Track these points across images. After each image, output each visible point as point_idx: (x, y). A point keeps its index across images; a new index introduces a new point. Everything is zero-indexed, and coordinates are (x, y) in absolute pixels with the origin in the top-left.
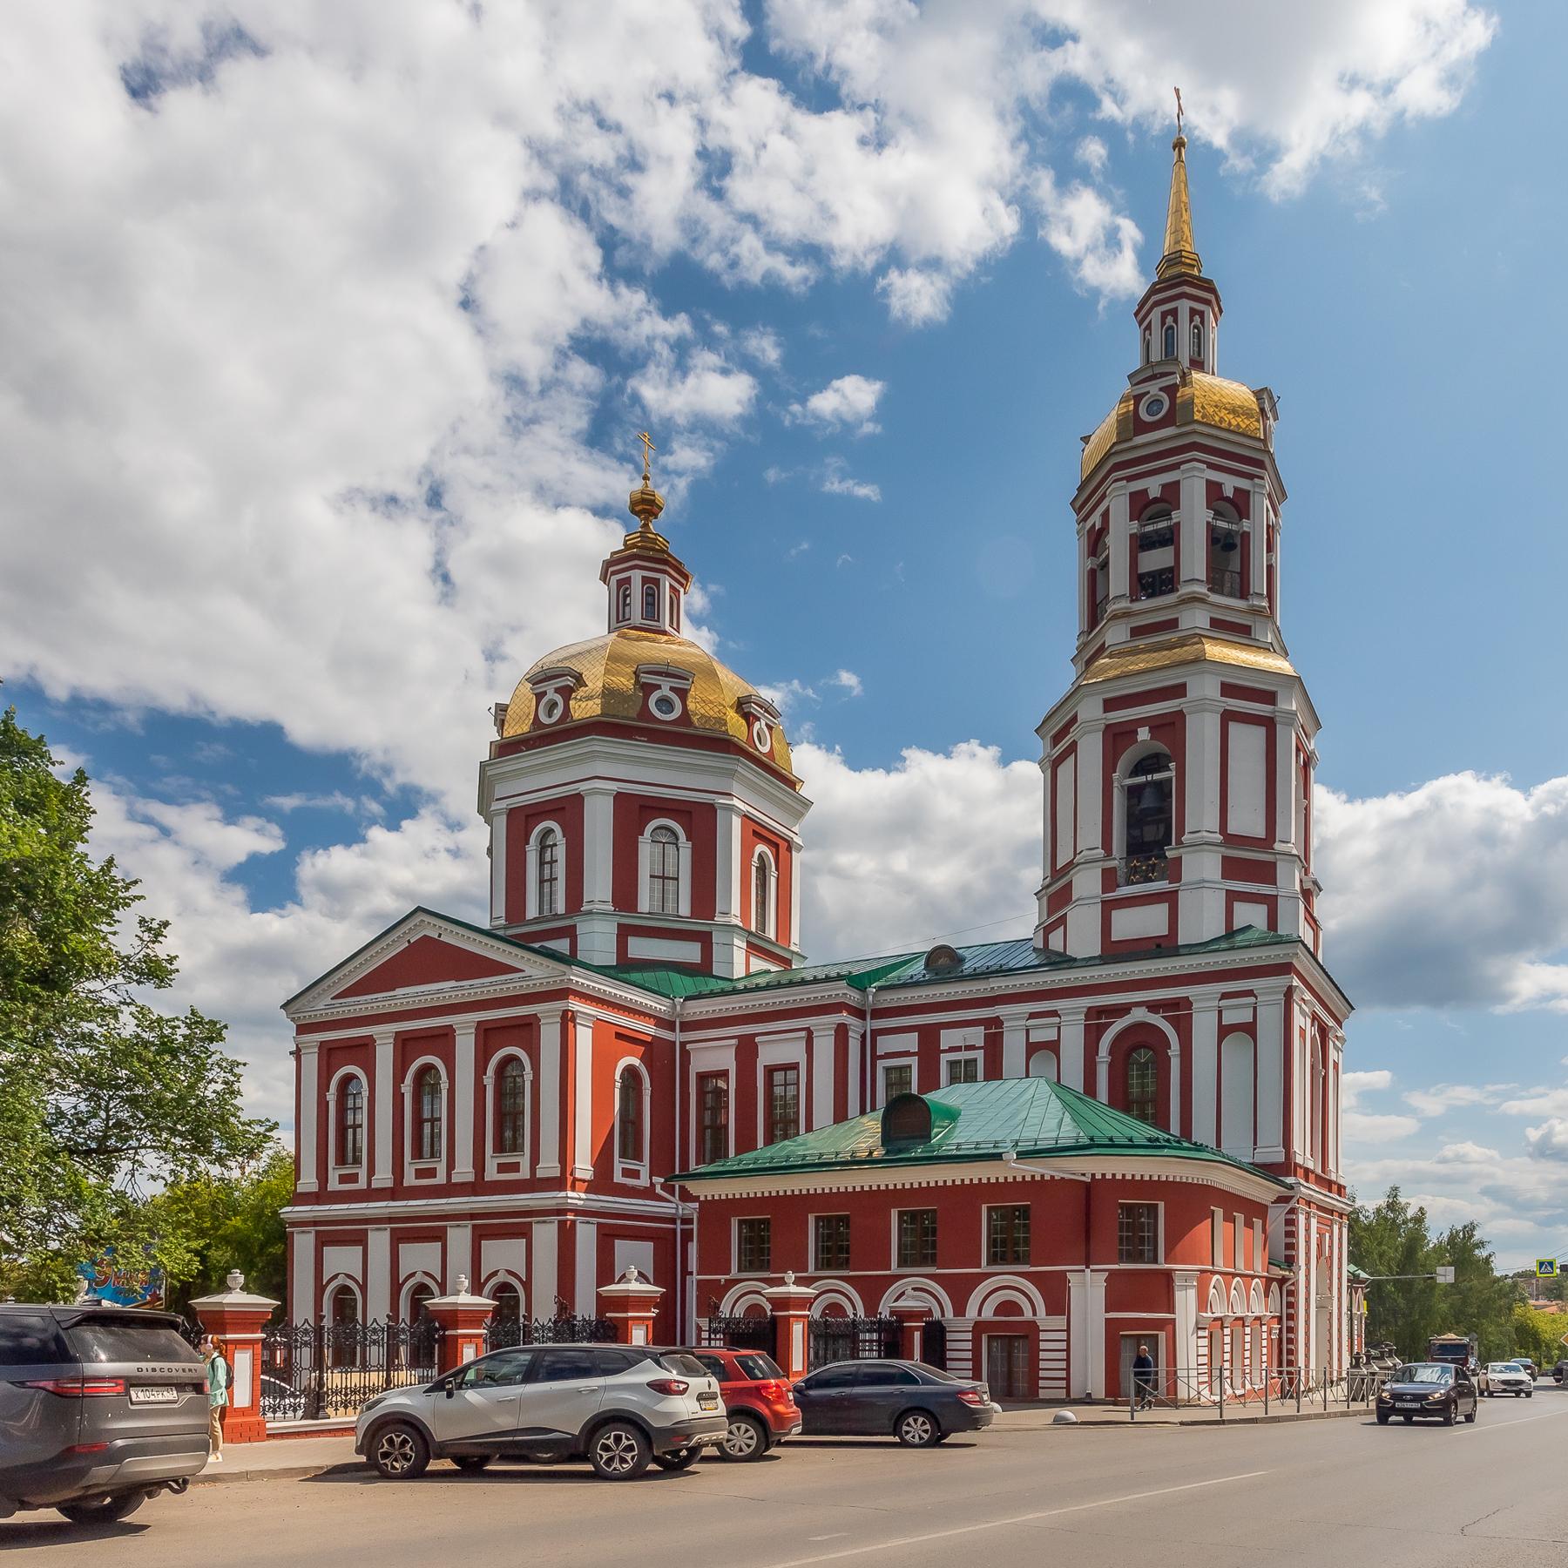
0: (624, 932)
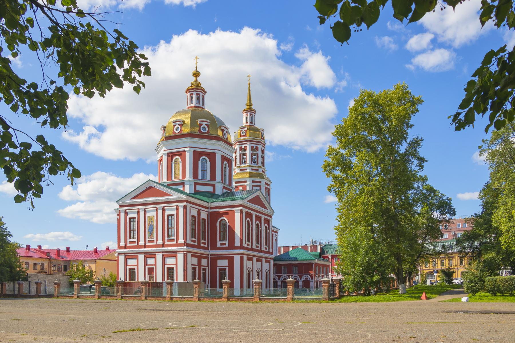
0: (196, 184)
